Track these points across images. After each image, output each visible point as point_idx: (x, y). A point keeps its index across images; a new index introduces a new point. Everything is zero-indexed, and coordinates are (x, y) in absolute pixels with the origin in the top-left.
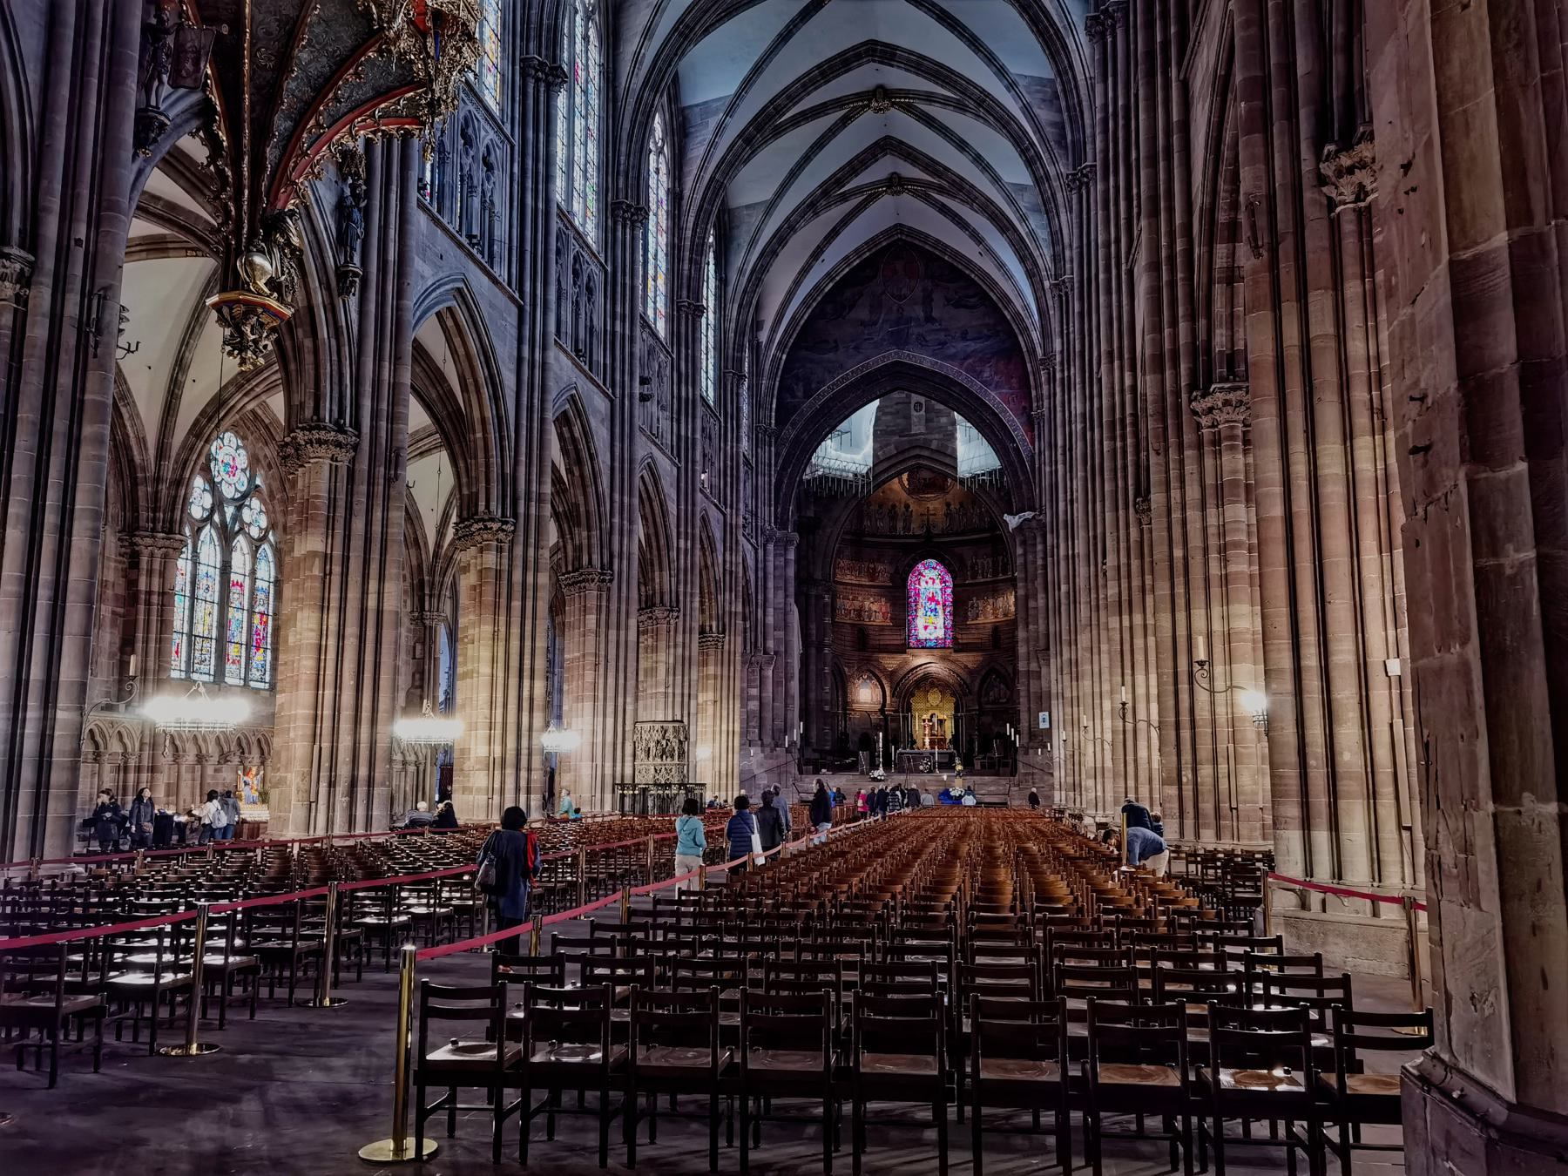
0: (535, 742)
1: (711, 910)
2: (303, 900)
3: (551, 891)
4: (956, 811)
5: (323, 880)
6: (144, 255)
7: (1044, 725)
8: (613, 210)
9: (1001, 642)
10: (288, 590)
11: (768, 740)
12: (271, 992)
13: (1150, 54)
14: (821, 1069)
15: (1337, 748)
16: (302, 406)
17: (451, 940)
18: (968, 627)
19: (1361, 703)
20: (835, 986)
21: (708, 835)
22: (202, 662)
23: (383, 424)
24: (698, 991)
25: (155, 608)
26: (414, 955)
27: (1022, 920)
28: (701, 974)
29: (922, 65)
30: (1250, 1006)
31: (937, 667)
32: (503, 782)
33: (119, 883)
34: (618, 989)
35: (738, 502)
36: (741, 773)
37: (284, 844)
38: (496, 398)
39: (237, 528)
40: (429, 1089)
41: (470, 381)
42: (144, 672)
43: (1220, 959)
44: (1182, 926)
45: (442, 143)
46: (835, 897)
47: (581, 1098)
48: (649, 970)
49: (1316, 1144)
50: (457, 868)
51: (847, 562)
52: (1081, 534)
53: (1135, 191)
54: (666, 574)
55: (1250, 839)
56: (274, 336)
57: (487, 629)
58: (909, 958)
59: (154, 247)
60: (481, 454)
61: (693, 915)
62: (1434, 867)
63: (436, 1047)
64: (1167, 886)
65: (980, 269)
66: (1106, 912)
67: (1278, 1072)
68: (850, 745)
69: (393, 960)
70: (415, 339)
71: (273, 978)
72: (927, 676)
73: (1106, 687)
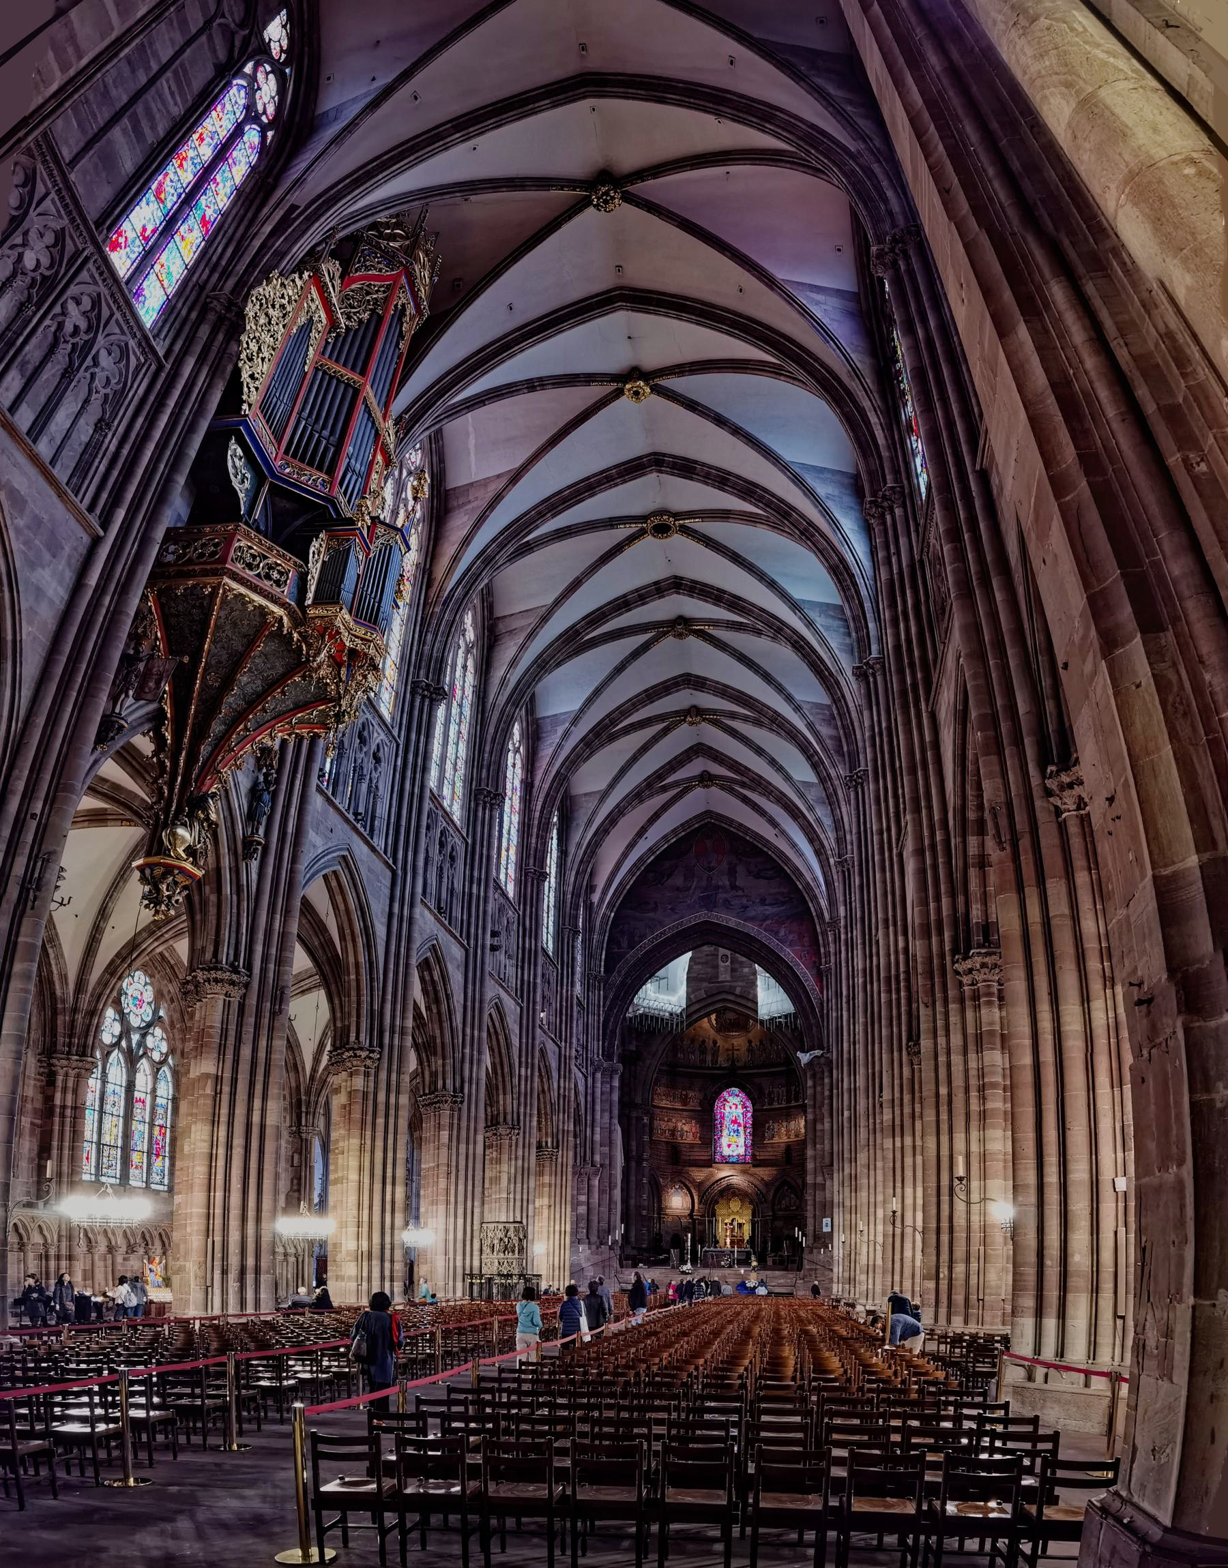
0: (396, 1238)
1: (546, 1377)
2: (207, 1366)
3: (414, 1361)
4: (750, 1300)
5: (222, 1351)
6: (86, 824)
7: (826, 1229)
8: (476, 795)
9: (793, 1157)
10: (183, 1106)
11: (594, 1238)
12: (188, 1439)
13: (903, 693)
14: (635, 1499)
15: (1070, 1250)
16: (203, 949)
17: (332, 1400)
18: (765, 1146)
19: (1092, 1214)
20: (647, 1437)
21: (544, 1317)
22: (109, 1167)
23: (272, 966)
24: (537, 1440)
25: (68, 1120)
26: (303, 1411)
27: (801, 1387)
28: (538, 1427)
30: (977, 1455)
31: (737, 1179)
32: (370, 1272)
33: (50, 1352)
34: (472, 1439)
35: (571, 1037)
36: (571, 1266)
37: (187, 1321)
38: (369, 946)
39: (141, 1053)
40: (324, 1513)
41: (347, 931)
42: (60, 1175)
43: (958, 1419)
44: (930, 1393)
45: (342, 742)
46: (648, 1368)
47: (446, 1520)
48: (496, 1425)
49: (1014, 1551)
50: (333, 1342)
51: (663, 1089)
52: (861, 1070)
53: (900, 791)
54: (509, 1097)
55: (992, 1324)
56: (186, 893)
57: (355, 1142)
58: (707, 1417)
59: (96, 818)
60: (353, 993)
61: (532, 1381)
62: (1140, 1348)
63: (327, 1482)
64: (920, 1362)
65: (776, 847)
66: (870, 1381)
67: (992, 1504)
68: (663, 1244)
69: (286, 1415)
70: (304, 897)
71: (188, 1428)
72: (729, 1187)
73: (880, 1198)
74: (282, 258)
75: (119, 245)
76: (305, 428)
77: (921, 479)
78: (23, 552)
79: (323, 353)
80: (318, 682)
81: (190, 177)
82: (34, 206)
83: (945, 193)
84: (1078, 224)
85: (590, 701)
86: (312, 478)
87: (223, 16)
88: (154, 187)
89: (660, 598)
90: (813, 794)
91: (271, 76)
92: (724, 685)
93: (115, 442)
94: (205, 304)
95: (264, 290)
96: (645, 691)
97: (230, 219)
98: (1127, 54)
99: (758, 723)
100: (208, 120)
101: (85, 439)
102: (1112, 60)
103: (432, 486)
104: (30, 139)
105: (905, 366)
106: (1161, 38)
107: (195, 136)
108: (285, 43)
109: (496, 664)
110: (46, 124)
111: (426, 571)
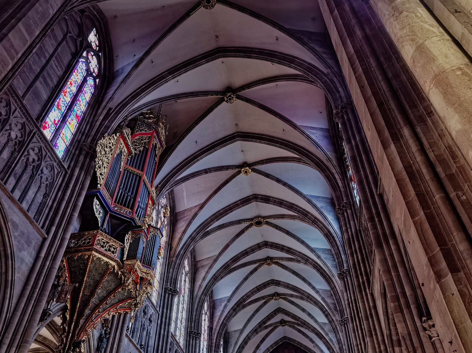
13: (359, 285)
29: (289, 286)
53: (363, 327)
74: (108, 129)
75: (46, 127)
76: (122, 192)
77: (357, 199)
78: (17, 245)
79: (127, 164)
80: (128, 291)
81: (69, 99)
82: (12, 114)
83: (362, 87)
84: (414, 97)
85: (234, 292)
86: (125, 211)
87: (70, 33)
88: (56, 104)
89: (260, 250)
90: (328, 328)
91: (94, 57)
92: (287, 284)
93: (51, 202)
94: (81, 148)
95: (102, 141)
96: (256, 287)
97: (87, 115)
98: (438, 25)
99: (302, 298)
100: (72, 76)
101: (40, 201)
102: (431, 28)
103: (170, 212)
104: (5, 88)
105: (348, 156)
106: (453, 17)
107: (69, 83)
108: (97, 43)
109: (197, 280)
110: (10, 82)
111: (169, 244)
